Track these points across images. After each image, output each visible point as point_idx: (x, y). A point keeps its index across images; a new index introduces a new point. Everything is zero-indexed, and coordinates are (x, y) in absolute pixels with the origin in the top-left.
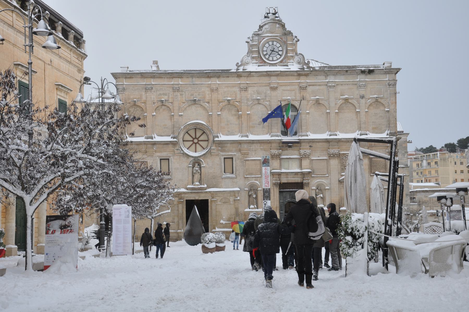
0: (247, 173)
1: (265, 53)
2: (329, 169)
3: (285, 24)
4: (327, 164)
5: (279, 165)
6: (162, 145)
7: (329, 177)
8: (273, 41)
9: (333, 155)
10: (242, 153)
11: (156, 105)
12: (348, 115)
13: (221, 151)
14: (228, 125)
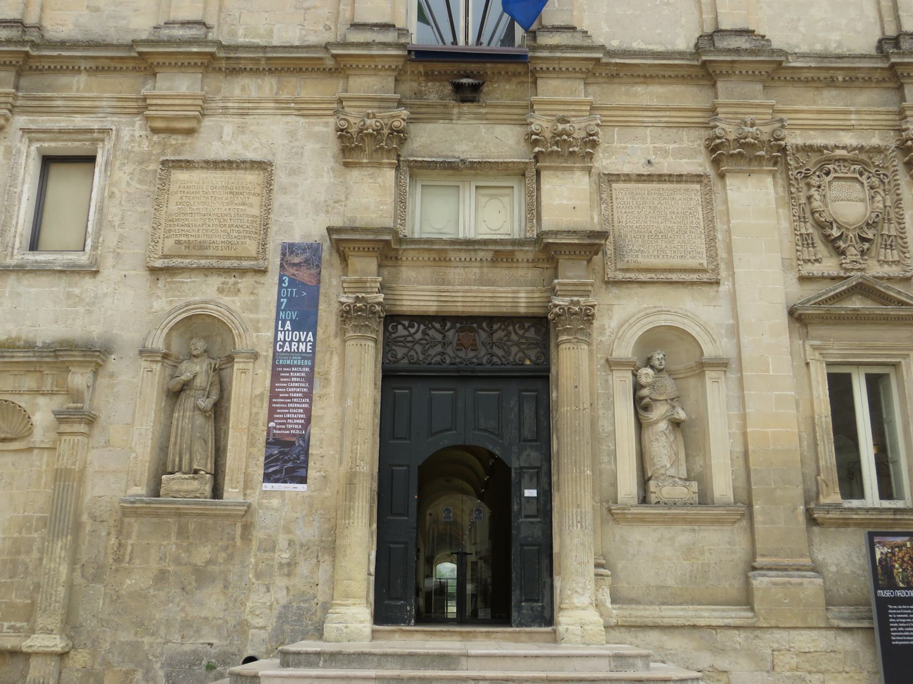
0: (170, 242)
2: (720, 236)
4: (708, 203)
5: (390, 199)
7: (724, 288)
9: (742, 146)
10: (154, 118)
13: (26, 111)
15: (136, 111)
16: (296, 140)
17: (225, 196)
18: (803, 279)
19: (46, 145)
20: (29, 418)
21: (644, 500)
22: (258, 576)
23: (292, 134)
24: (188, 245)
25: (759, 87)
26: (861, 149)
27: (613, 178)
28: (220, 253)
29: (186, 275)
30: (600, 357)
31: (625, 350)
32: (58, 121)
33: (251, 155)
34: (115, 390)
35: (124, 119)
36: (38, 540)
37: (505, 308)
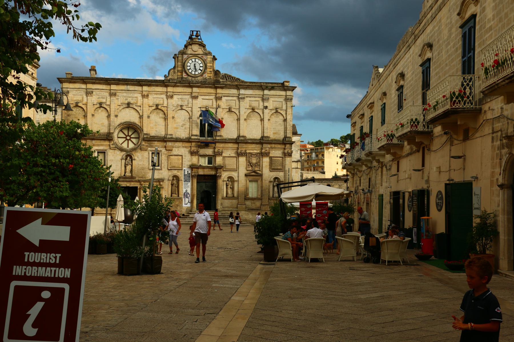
0: (171, 166)
1: (188, 68)
3: (205, 45)
4: (237, 160)
6: (100, 141)
8: (196, 59)
11: (96, 106)
12: (255, 121)
13: (150, 147)
14: (156, 125)
18: (247, 170)
21: (227, 196)
23: (185, 151)
24: (173, 166)
26: (256, 153)
27: (225, 157)
30: (222, 180)
31: (226, 179)
33: (180, 154)
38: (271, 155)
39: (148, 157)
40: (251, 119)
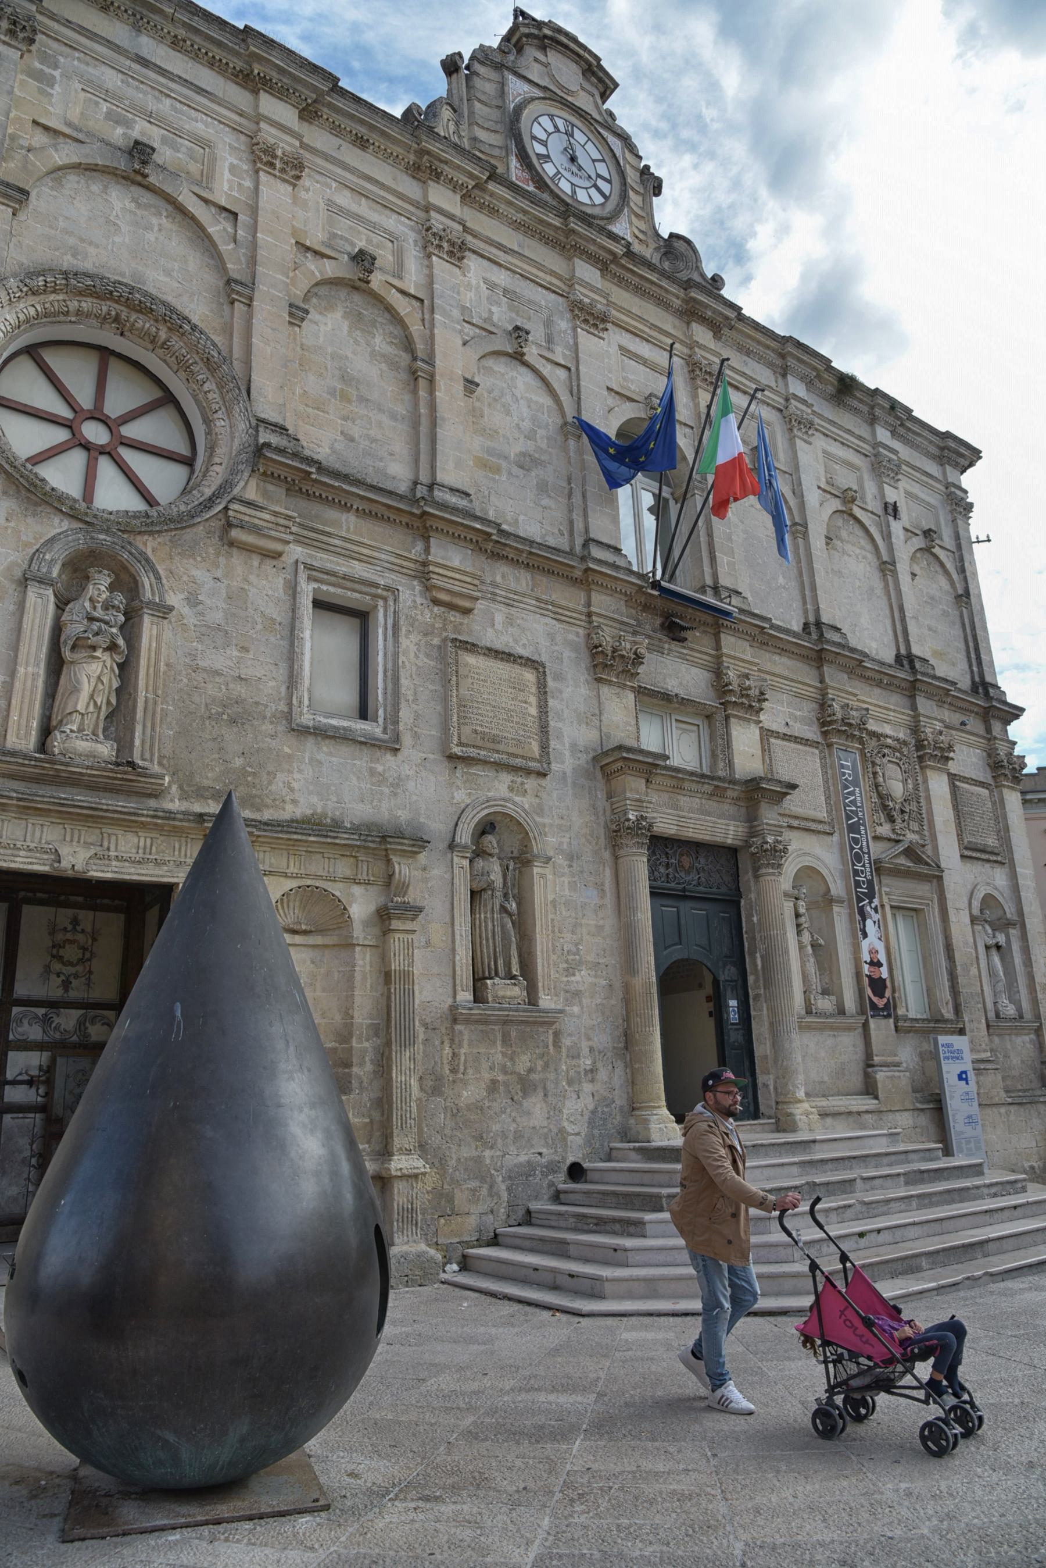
13: (300, 541)
14: (344, 397)
15: (413, 573)
16: (556, 644)
17: (510, 690)
19: (324, 588)
20: (345, 909)
21: (809, 1012)
22: (570, 1083)
23: (551, 637)
25: (846, 676)
28: (511, 750)
29: (479, 767)
32: (338, 564)
34: (429, 885)
35: (404, 580)
36: (370, 1050)
37: (719, 839)
38: (953, 767)
39: (278, 613)
40: (844, 552)
